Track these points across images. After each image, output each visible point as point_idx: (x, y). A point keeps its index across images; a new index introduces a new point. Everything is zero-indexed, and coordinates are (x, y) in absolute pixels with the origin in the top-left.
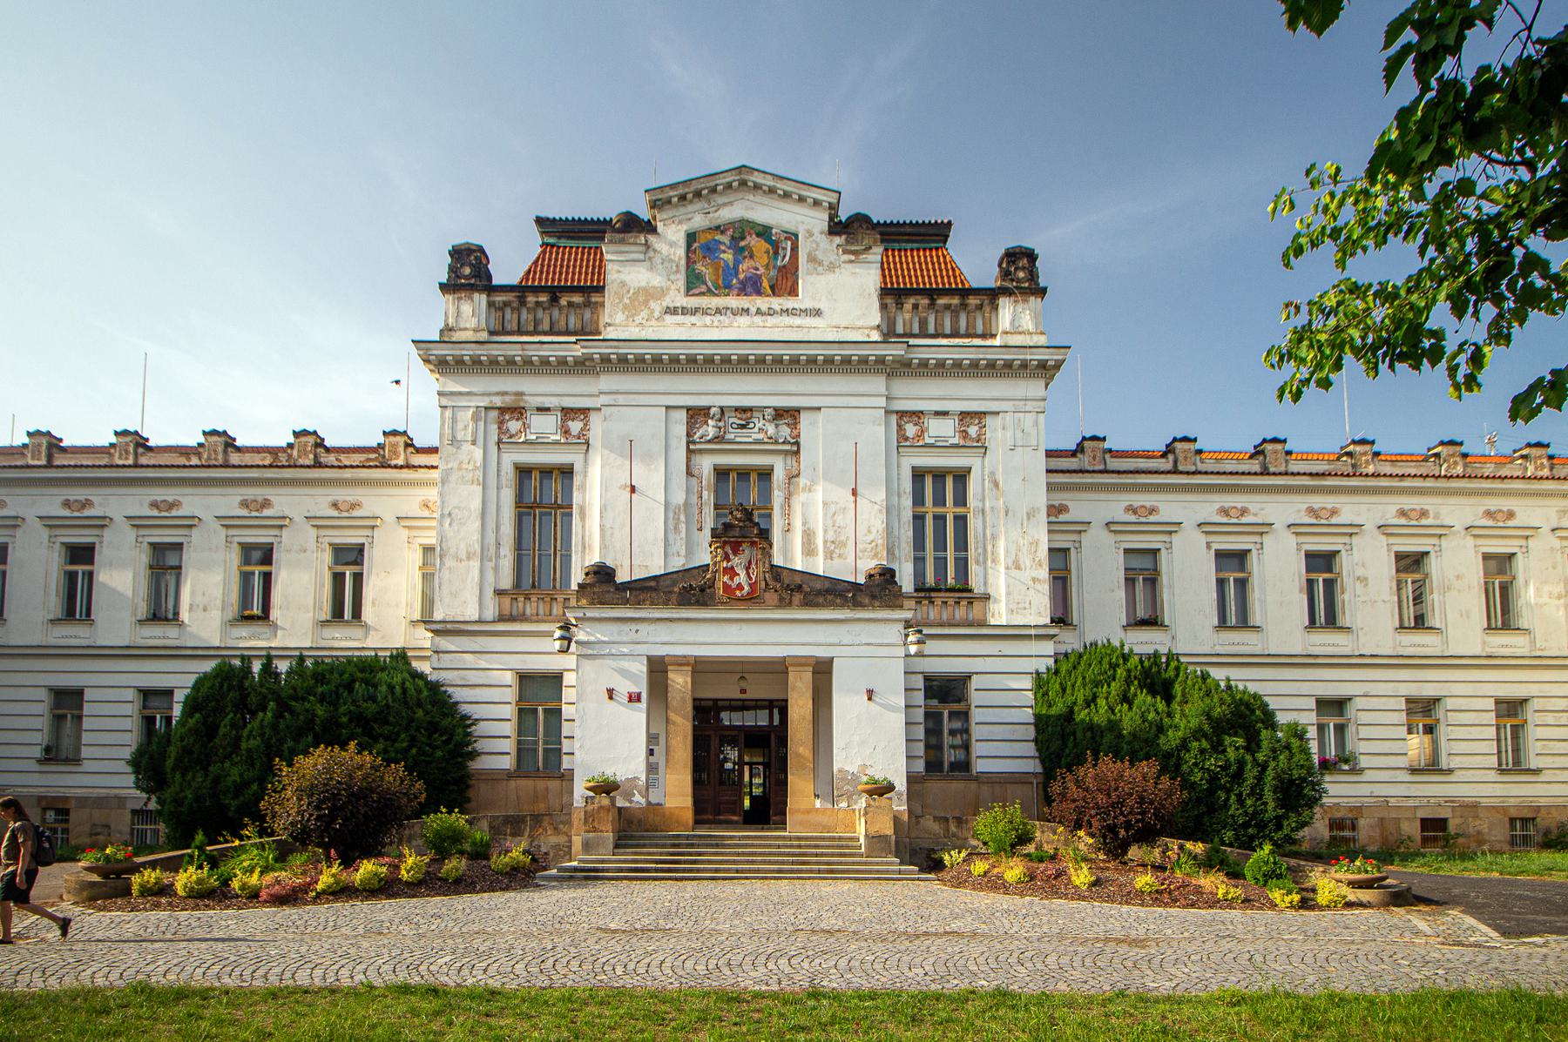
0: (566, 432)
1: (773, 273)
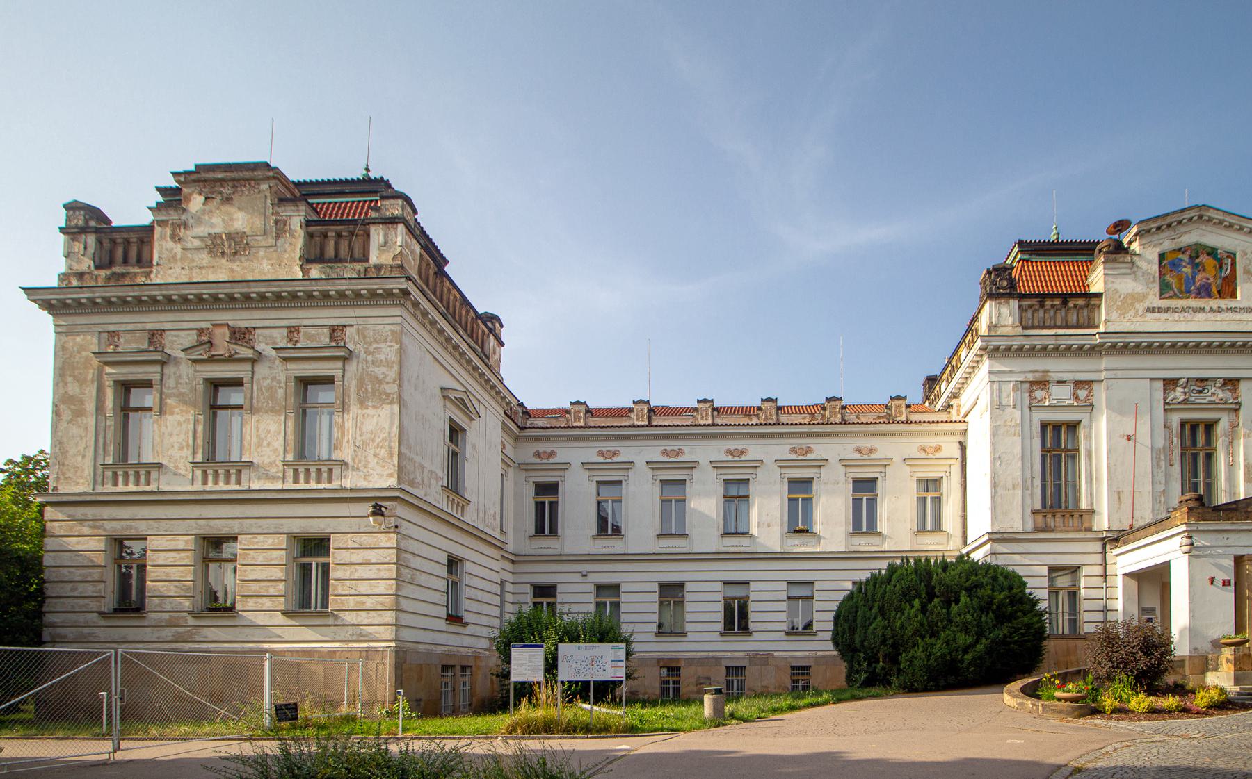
0: (1077, 398)
1: (1219, 282)
